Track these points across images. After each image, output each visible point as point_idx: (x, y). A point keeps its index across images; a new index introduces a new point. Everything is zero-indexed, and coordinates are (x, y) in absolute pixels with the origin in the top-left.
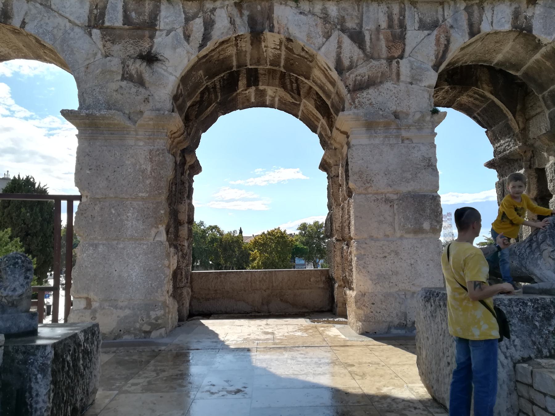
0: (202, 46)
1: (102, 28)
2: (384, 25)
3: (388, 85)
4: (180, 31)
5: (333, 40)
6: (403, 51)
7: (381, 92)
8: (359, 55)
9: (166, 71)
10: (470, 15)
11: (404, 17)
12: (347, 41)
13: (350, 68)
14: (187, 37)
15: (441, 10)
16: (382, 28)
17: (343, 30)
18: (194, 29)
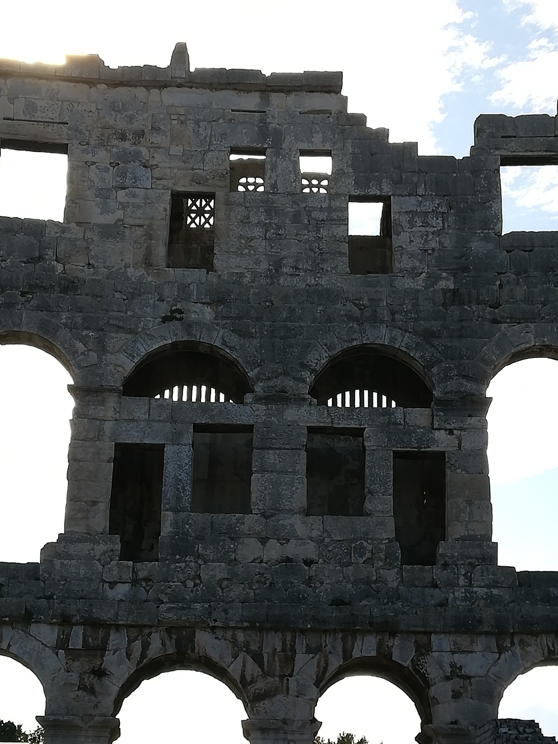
0: (139, 663)
1: (66, 649)
2: (279, 649)
3: (280, 697)
4: (124, 651)
5: (240, 659)
6: (293, 670)
7: (273, 703)
8: (258, 672)
9: (111, 682)
10: (345, 643)
11: (295, 643)
12: (250, 660)
13: (252, 682)
14: (128, 656)
15: (325, 637)
16: (277, 651)
17: (248, 651)
18: (134, 649)
